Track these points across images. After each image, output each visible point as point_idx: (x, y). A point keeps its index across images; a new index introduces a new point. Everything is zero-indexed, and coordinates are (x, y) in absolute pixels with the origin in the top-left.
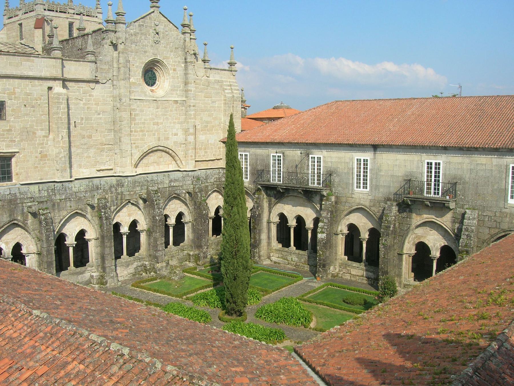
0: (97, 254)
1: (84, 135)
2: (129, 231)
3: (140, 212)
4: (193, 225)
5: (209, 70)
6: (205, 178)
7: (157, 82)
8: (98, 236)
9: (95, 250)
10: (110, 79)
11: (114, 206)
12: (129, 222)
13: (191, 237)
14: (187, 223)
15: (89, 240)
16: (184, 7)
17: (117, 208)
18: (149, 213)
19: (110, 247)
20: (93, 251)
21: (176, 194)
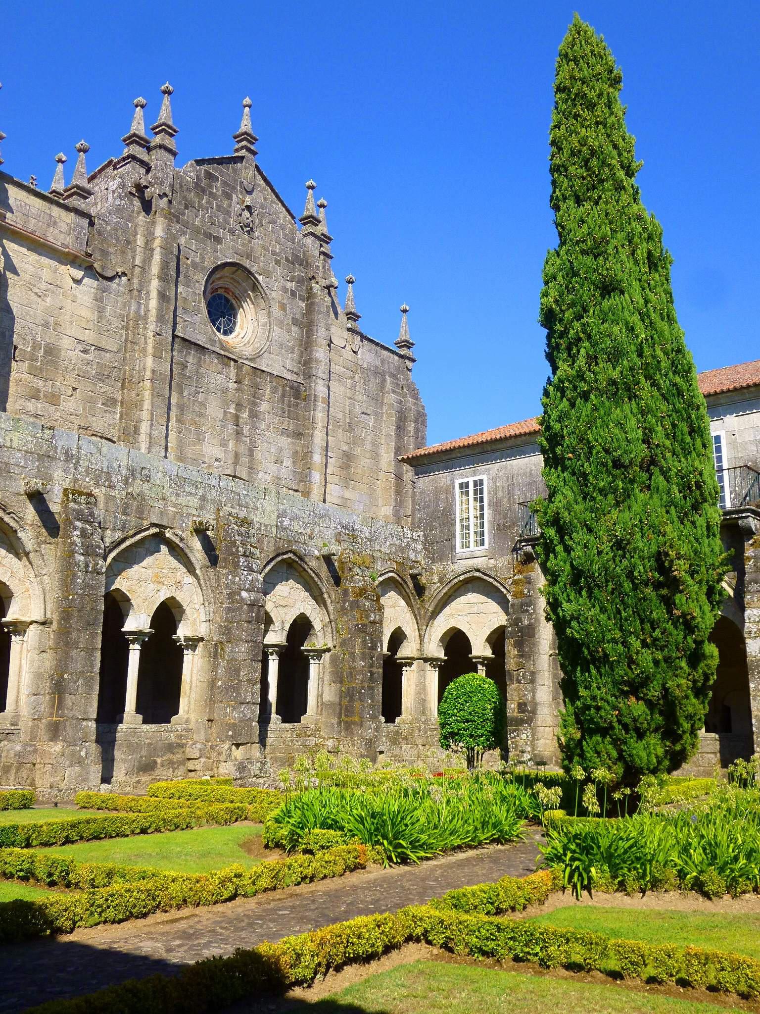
0: (38, 676)
1: (38, 391)
2: (153, 631)
3: (190, 579)
4: (334, 661)
5: (358, 338)
6: (368, 535)
7: (237, 328)
8: (49, 616)
9: (32, 661)
10: (124, 274)
11: (115, 530)
12: (154, 602)
13: (330, 694)
14: (319, 653)
15: (19, 628)
16: (308, 183)
17: (123, 540)
18: (219, 586)
19: (90, 651)
20: (25, 668)
21: (295, 554)
